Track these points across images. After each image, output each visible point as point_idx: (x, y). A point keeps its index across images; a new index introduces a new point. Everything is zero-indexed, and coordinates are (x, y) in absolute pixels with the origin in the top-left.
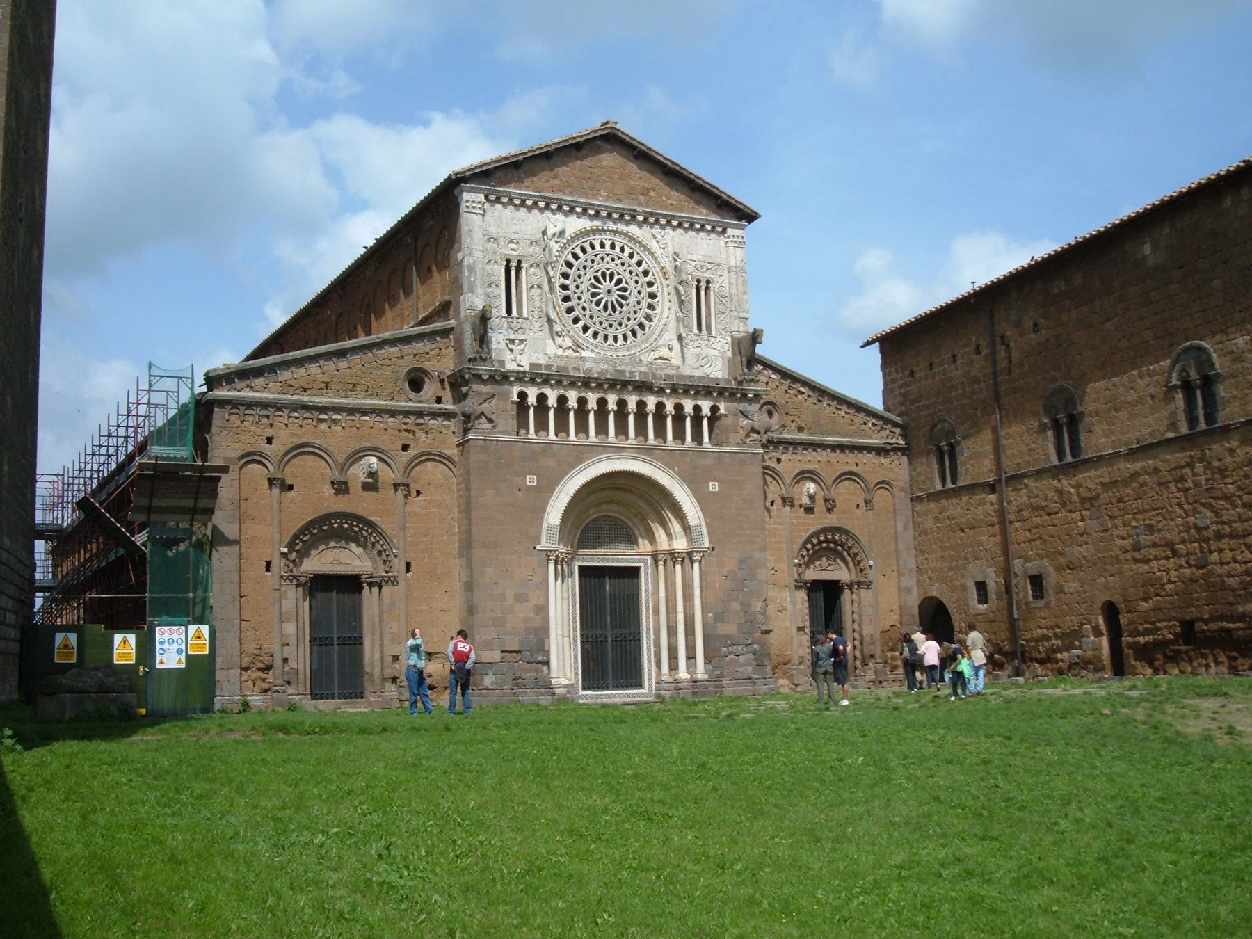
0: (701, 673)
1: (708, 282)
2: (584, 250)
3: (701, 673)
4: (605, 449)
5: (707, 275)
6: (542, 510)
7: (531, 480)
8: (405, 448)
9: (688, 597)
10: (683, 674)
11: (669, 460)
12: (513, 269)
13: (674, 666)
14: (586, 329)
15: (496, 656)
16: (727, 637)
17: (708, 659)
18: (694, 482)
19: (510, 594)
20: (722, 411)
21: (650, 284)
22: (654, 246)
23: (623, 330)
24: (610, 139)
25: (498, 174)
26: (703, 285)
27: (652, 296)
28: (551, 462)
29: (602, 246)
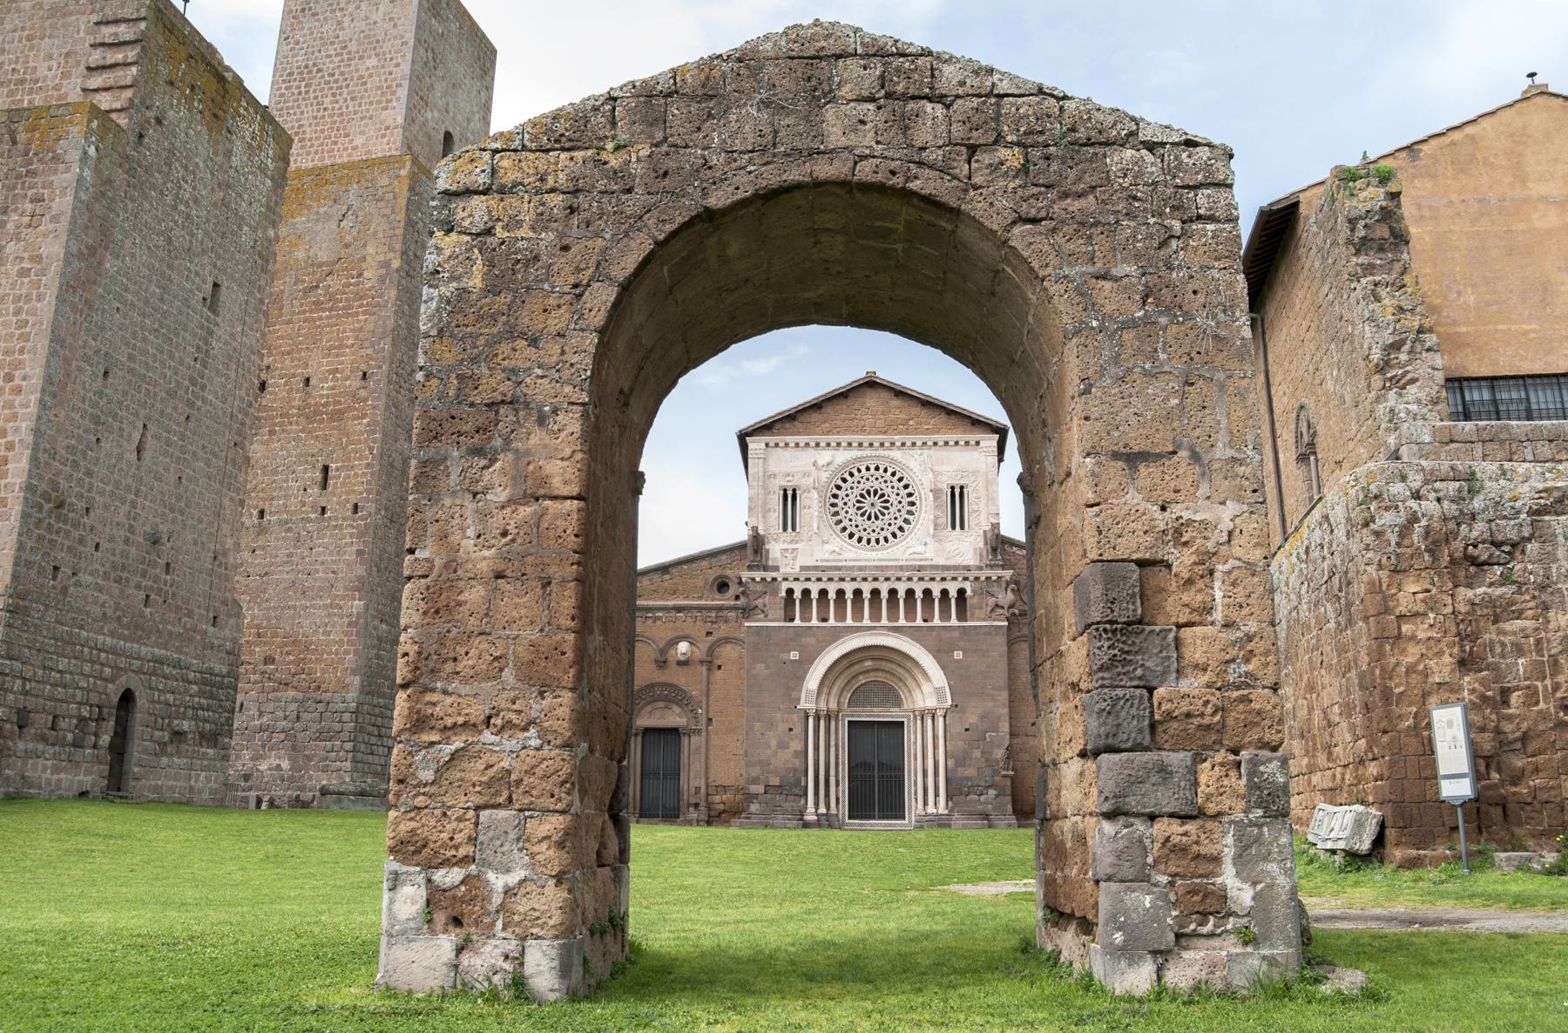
0: (942, 809)
1: (962, 488)
2: (851, 475)
3: (942, 809)
4: (859, 629)
5: (962, 482)
6: (801, 678)
7: (794, 655)
8: (709, 634)
9: (935, 747)
10: (931, 809)
11: (913, 633)
12: (790, 497)
13: (925, 803)
14: (851, 536)
15: (760, 789)
16: (968, 778)
17: (949, 797)
18: (941, 653)
19: (774, 743)
20: (969, 592)
21: (910, 495)
22: (912, 464)
23: (883, 533)
24: (871, 384)
25: (778, 426)
26: (957, 491)
27: (913, 504)
28: (811, 640)
29: (868, 469)
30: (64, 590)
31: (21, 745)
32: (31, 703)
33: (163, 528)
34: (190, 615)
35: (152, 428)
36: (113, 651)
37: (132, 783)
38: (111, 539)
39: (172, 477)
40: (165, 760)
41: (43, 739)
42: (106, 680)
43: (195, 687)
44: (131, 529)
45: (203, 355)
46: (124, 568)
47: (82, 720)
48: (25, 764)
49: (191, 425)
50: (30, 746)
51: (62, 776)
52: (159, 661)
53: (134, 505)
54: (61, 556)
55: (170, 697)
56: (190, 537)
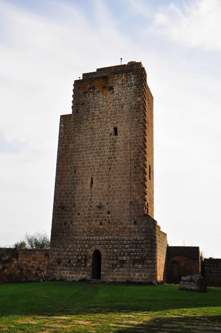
30: (69, 228)
31: (59, 268)
32: (61, 257)
33: (104, 203)
34: (122, 224)
35: (94, 178)
36: (87, 240)
37: (101, 277)
38: (83, 211)
39: (106, 187)
40: (115, 270)
41: (65, 265)
42: (87, 248)
43: (127, 246)
44: (91, 206)
45: (113, 149)
46: (89, 217)
47: (79, 261)
48: (60, 272)
49: (112, 170)
50: (62, 268)
51: (74, 275)
52: (109, 240)
53: (91, 200)
54: (66, 220)
55: (115, 250)
56: (117, 201)
